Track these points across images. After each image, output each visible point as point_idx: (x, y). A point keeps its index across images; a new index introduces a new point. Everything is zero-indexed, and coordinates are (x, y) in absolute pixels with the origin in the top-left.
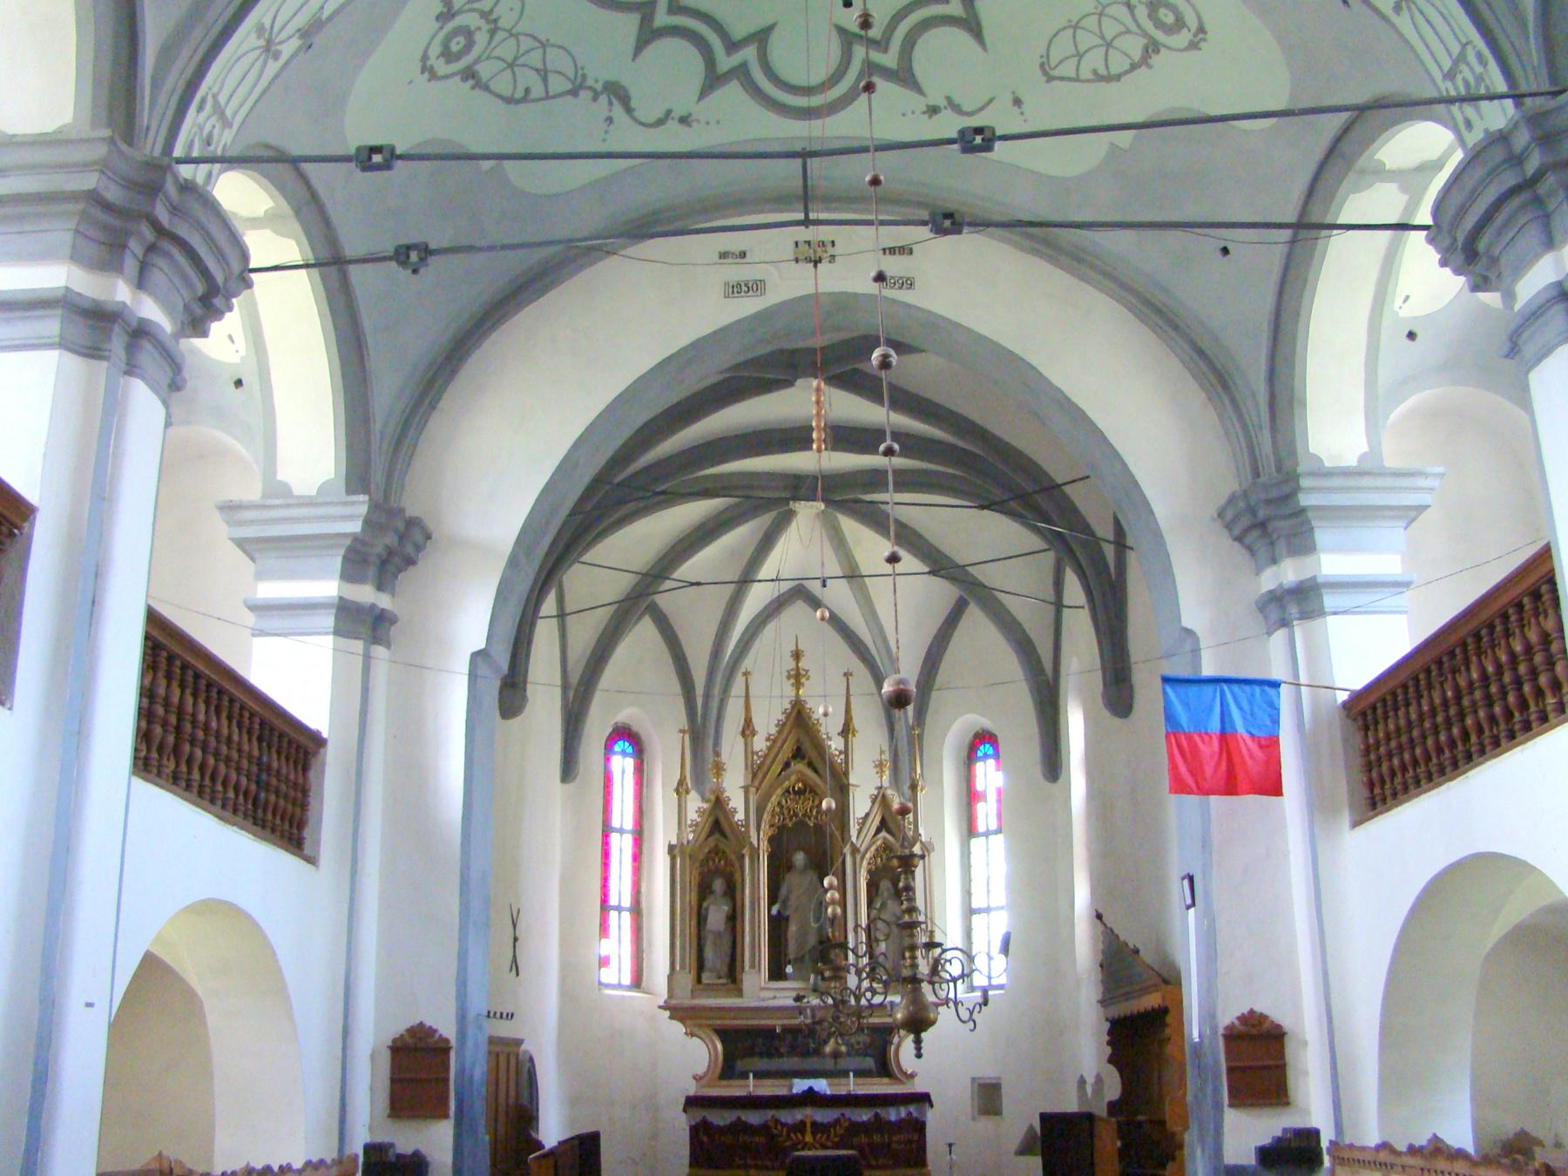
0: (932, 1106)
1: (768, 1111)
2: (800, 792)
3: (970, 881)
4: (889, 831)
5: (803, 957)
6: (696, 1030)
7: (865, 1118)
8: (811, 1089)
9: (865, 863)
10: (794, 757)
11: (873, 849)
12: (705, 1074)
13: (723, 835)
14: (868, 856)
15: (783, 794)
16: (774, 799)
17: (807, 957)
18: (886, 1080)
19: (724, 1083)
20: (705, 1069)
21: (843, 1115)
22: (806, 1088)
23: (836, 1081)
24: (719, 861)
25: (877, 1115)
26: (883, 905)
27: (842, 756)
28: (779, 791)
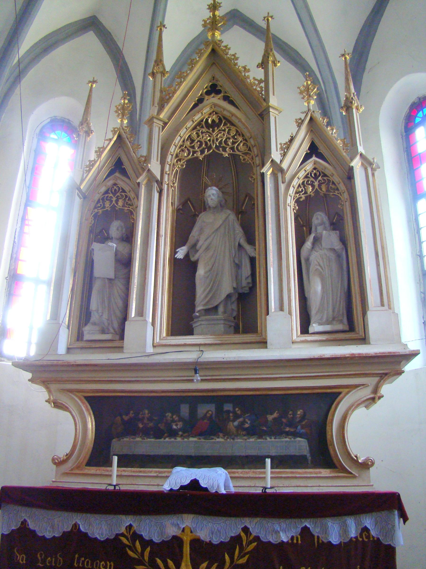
0: (404, 517)
1: (123, 517)
2: (214, 125)
3: (420, 243)
4: (320, 156)
5: (216, 308)
6: (64, 399)
7: (284, 538)
8: (195, 483)
9: (292, 191)
10: (208, 93)
11: (302, 174)
12: (69, 456)
13: (124, 172)
14: (296, 182)
15: (194, 128)
16: (184, 133)
17: (221, 309)
18: (325, 472)
19: (93, 470)
20: (68, 451)
21: (246, 530)
22: (186, 482)
23: (240, 472)
24: (117, 202)
25: (305, 530)
26: (317, 240)
27: (263, 85)
28: (190, 124)
